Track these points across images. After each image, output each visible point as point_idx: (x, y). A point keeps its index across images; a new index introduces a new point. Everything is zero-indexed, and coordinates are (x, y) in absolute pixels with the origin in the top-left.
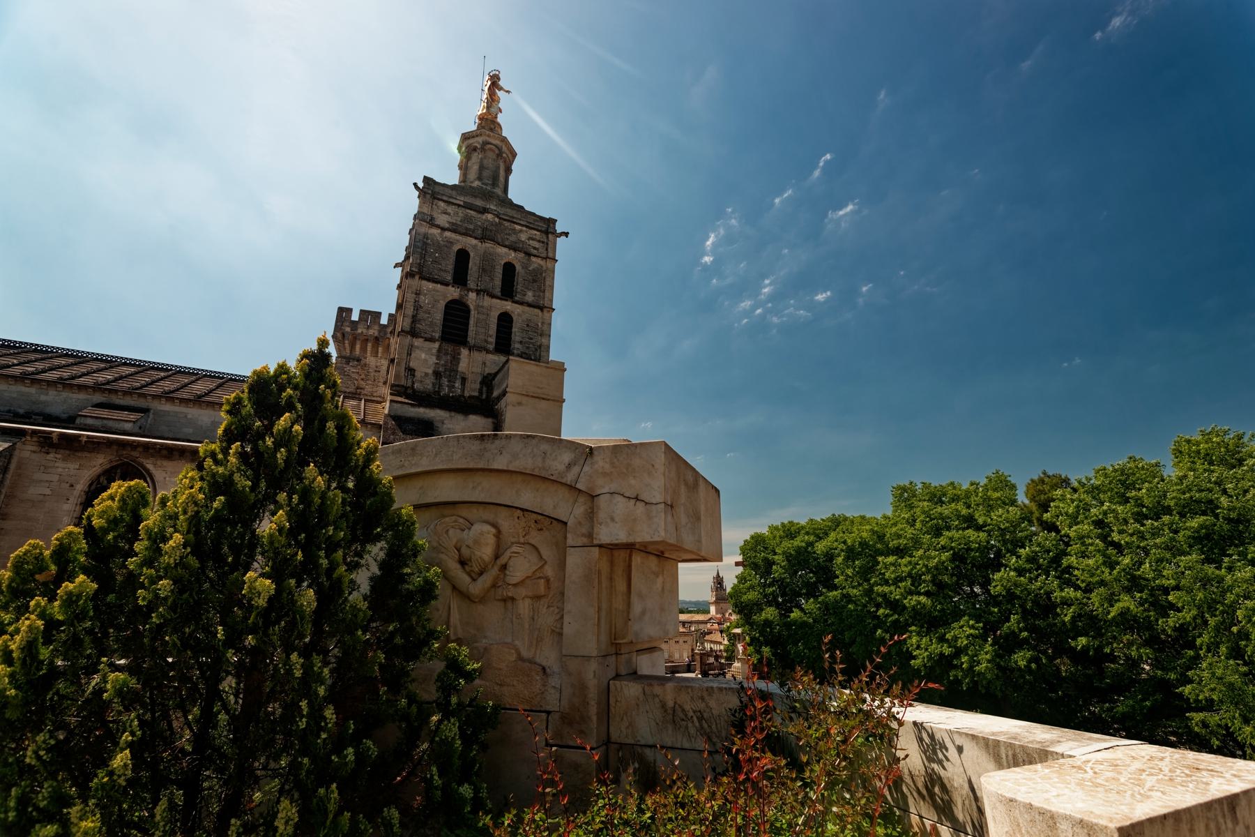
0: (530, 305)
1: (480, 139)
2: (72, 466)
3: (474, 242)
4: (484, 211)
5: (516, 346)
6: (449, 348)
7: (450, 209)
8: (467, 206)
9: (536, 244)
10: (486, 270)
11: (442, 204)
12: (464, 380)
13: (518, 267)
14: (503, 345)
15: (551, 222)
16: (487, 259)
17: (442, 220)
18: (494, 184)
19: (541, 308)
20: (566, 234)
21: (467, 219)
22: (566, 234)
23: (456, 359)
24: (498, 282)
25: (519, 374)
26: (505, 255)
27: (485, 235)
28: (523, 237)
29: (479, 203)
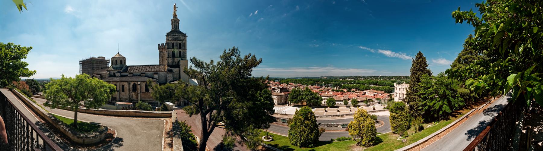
0: (183, 49)
1: (174, 20)
2: (144, 83)
3: (174, 41)
4: (175, 35)
5: (182, 56)
6: (173, 58)
7: (171, 37)
8: (173, 35)
9: (183, 39)
10: (177, 46)
11: (169, 36)
12: (175, 62)
13: (181, 44)
14: (180, 56)
15: (185, 34)
16: (176, 43)
17: (170, 39)
18: (177, 28)
19: (185, 49)
20: (188, 36)
21: (173, 38)
22: (188, 36)
23: (174, 60)
24: (178, 47)
25: (182, 63)
26: (179, 42)
27: (176, 40)
28: (181, 38)
29: (174, 34)
